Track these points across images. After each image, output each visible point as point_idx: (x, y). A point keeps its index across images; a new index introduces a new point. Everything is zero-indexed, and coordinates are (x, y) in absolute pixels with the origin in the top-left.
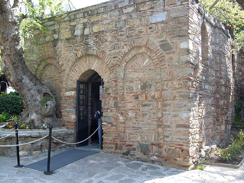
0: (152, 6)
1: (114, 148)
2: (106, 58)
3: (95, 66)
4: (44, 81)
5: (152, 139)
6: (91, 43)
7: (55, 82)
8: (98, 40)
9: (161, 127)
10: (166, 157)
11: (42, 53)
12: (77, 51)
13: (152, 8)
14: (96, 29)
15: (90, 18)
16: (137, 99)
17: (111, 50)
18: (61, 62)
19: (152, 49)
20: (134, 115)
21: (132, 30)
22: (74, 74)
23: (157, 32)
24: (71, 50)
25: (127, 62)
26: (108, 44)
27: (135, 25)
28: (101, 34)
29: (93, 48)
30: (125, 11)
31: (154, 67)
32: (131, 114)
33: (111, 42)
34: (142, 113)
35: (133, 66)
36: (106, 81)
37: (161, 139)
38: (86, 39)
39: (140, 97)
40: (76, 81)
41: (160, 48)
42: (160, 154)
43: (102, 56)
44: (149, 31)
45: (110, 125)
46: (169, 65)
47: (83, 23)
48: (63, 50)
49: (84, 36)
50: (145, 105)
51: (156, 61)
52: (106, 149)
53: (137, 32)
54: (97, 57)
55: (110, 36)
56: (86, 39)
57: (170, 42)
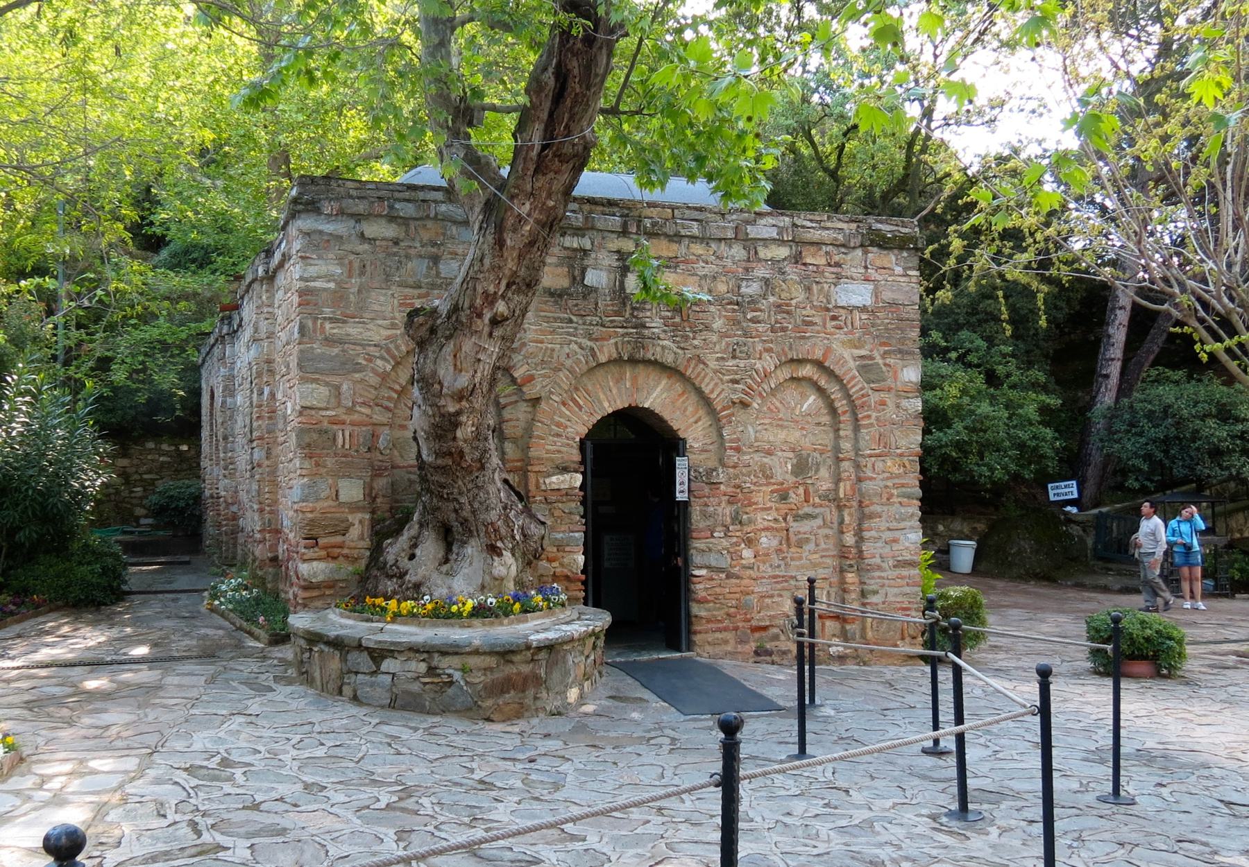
0: (836, 258)
1: (732, 642)
2: (707, 380)
3: (657, 396)
6: (655, 324)
12: (597, 340)
13: (838, 265)
16: (785, 499)
17: (723, 358)
19: (837, 372)
20: (775, 543)
23: (851, 332)
24: (569, 334)
26: (715, 338)
29: (661, 343)
30: (764, 253)
32: (765, 541)
33: (724, 335)
40: (578, 439)
44: (830, 324)
45: (723, 576)
46: (877, 419)
47: (618, 252)
50: (808, 516)
52: (708, 648)
54: (672, 371)
56: (634, 309)
57: (881, 362)
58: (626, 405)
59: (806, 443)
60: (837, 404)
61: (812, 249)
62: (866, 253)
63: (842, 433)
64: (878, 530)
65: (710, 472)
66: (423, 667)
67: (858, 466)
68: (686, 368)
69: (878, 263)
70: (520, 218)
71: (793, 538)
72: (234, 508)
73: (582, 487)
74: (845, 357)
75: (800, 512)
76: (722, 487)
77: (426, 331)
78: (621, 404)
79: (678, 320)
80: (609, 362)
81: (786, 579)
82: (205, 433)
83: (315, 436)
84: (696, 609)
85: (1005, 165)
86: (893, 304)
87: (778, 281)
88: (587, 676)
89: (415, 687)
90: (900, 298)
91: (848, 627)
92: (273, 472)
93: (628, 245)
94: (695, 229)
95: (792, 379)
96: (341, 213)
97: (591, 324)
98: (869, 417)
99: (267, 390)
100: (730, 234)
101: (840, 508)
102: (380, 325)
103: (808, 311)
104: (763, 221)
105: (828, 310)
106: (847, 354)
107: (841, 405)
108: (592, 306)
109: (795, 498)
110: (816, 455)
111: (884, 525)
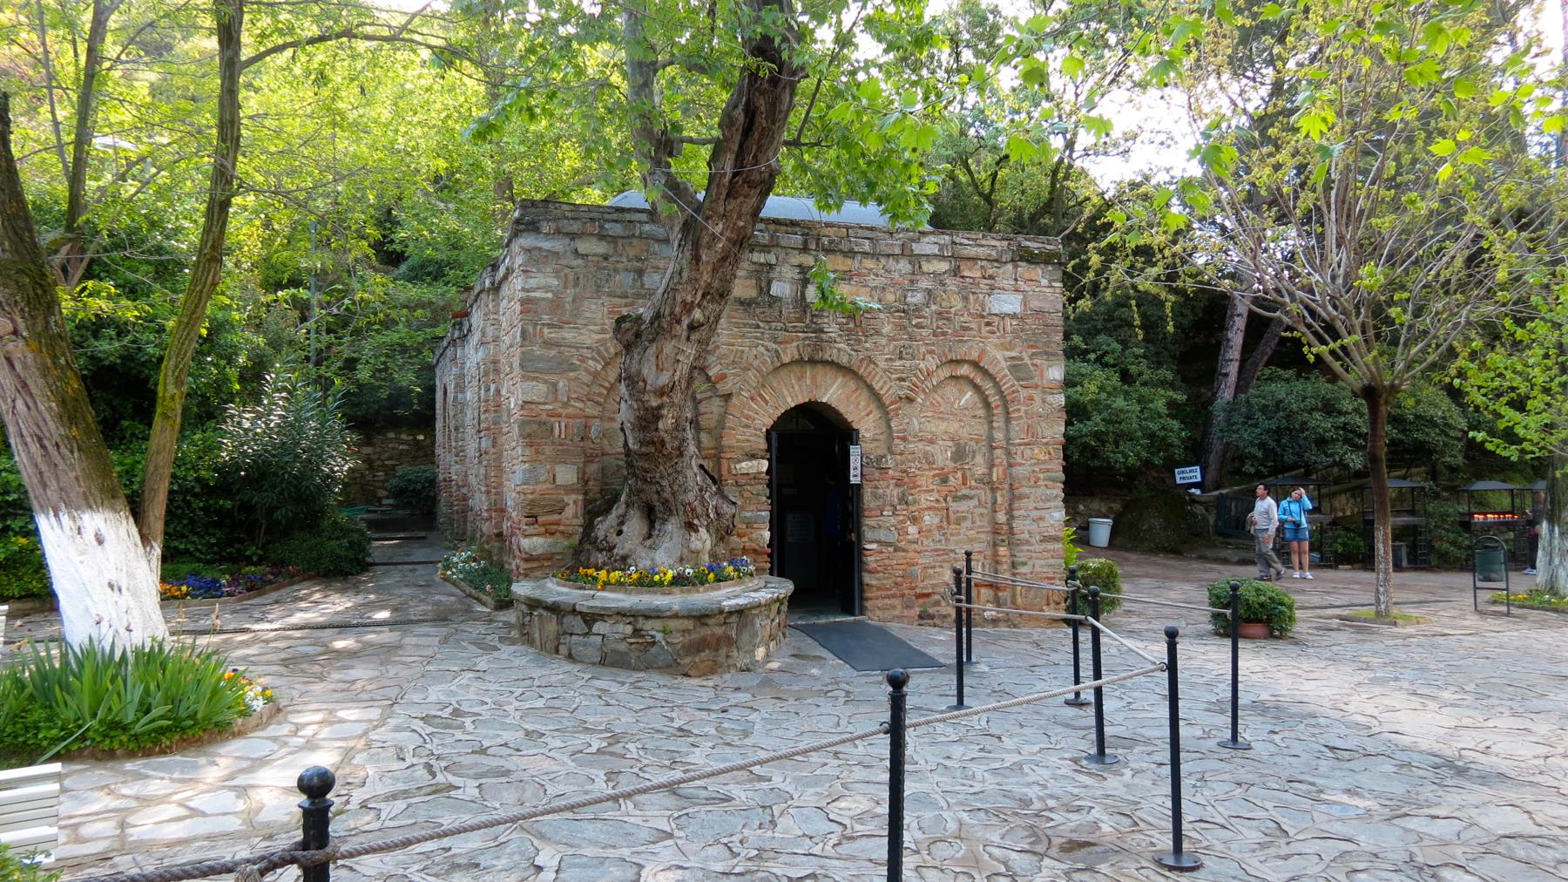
0: (990, 272)
3: (834, 393)
6: (832, 329)
8: (851, 325)
20: (937, 520)
26: (884, 342)
30: (926, 267)
32: (929, 519)
44: (985, 329)
50: (966, 497)
52: (878, 612)
59: (964, 433)
60: (991, 399)
61: (969, 263)
62: (1016, 267)
64: (1027, 509)
66: (629, 629)
67: (1009, 454)
69: (1027, 276)
70: (714, 237)
71: (952, 517)
72: (464, 490)
73: (769, 472)
74: (998, 358)
77: (632, 335)
79: (851, 325)
80: (792, 362)
81: (946, 552)
82: (439, 425)
83: (535, 427)
84: (867, 578)
85: (1137, 190)
86: (1039, 312)
87: (939, 292)
88: (772, 638)
89: (623, 647)
90: (1046, 306)
92: (499, 458)
93: (808, 260)
94: (867, 246)
96: (558, 232)
99: (493, 387)
100: (897, 251)
101: (993, 490)
102: (591, 330)
103: (966, 318)
104: (926, 240)
106: (1000, 355)
107: (994, 400)
108: (776, 314)
111: (1032, 505)
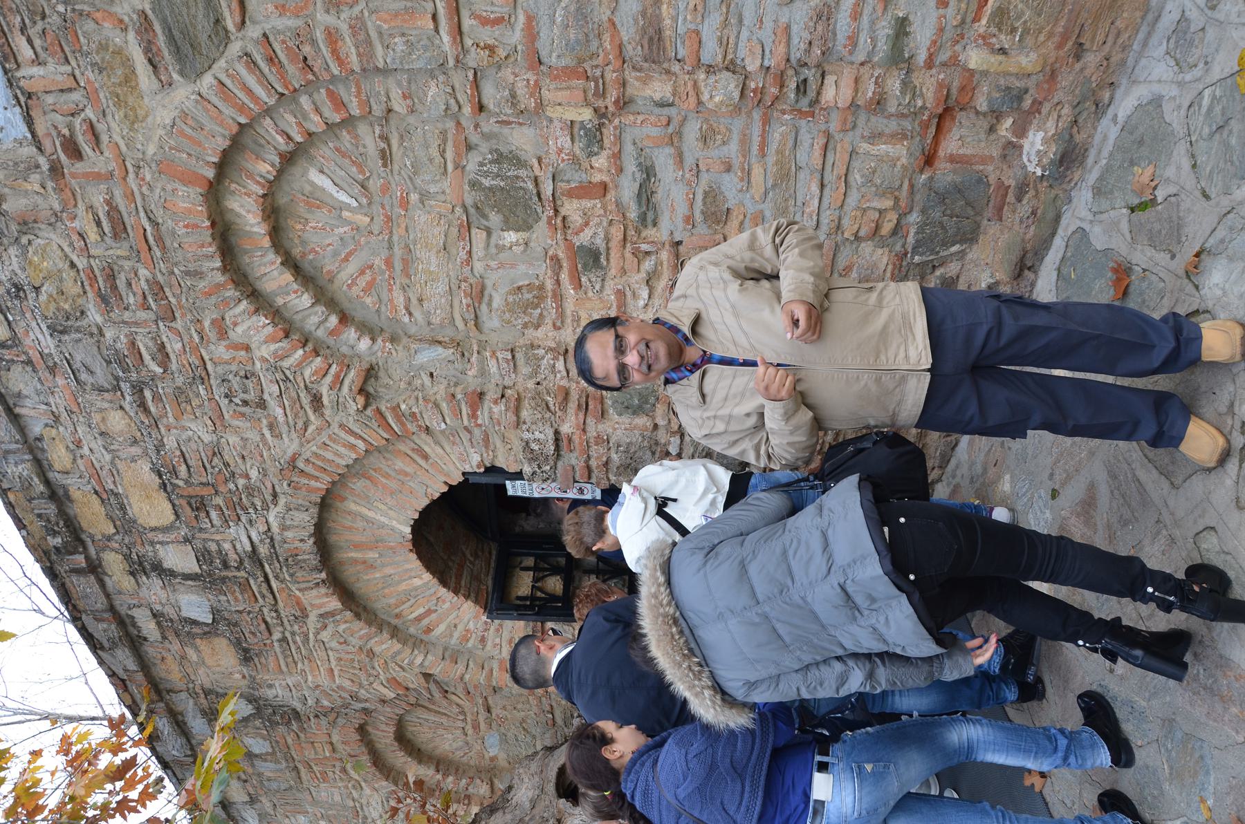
2: (329, 456)
3: (384, 518)
4: (492, 759)
5: (893, 162)
7: (496, 711)
9: (812, 86)
10: (1060, 46)
11: (344, 770)
14: (153, 510)
15: (92, 537)
17: (271, 427)
18: (381, 688)
21: (114, 288)
22: (448, 627)
25: (344, 319)
27: (73, 265)
28: (181, 483)
29: (275, 529)
31: (363, 129)
34: (702, 229)
35: (368, 276)
36: (476, 458)
37: (905, 84)
38: (226, 565)
39: (584, 238)
41: (208, 79)
42: (1020, 99)
43: (317, 479)
44: (95, 161)
47: (132, 574)
48: (310, 678)
49: (210, 575)
50: (646, 195)
51: (317, 110)
53: (121, 250)
55: (184, 429)
58: (413, 556)
63: (399, 106)
65: (533, 457)
68: (311, 490)
75: (633, 214)
76: (566, 429)
78: (413, 562)
91: (982, 104)
93: (113, 562)
95: (276, 234)
97: (279, 617)
98: (332, 37)
101: (624, 104)
105: (56, 170)
109: (590, 223)
110: (472, 162)
